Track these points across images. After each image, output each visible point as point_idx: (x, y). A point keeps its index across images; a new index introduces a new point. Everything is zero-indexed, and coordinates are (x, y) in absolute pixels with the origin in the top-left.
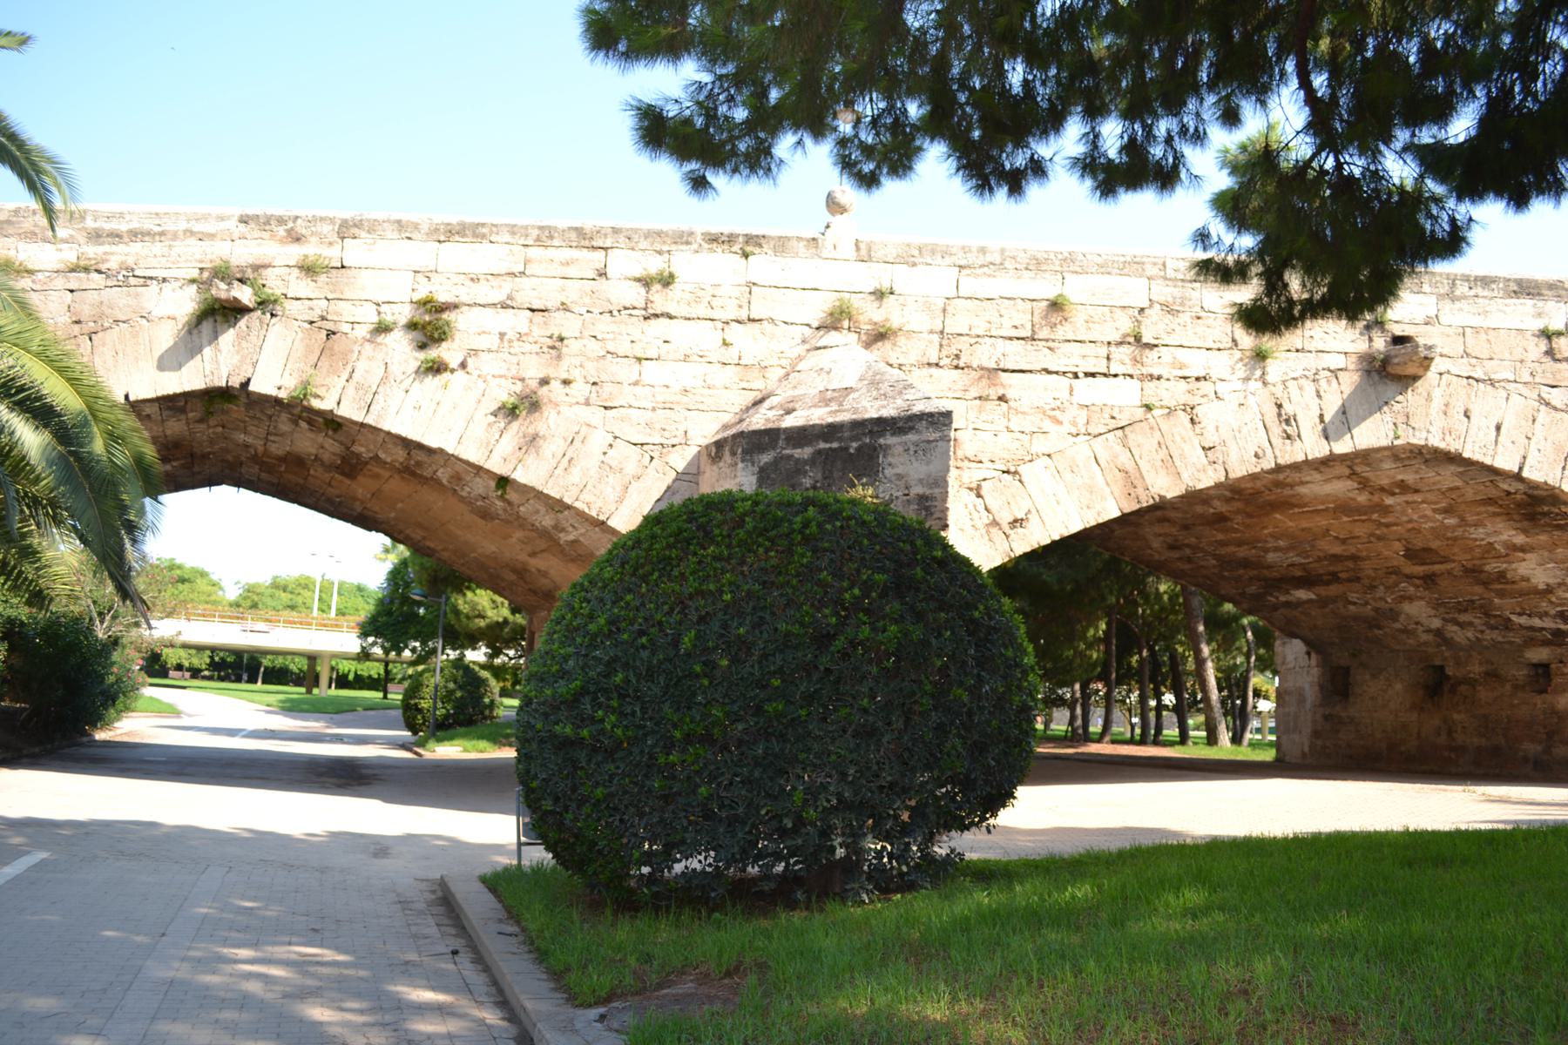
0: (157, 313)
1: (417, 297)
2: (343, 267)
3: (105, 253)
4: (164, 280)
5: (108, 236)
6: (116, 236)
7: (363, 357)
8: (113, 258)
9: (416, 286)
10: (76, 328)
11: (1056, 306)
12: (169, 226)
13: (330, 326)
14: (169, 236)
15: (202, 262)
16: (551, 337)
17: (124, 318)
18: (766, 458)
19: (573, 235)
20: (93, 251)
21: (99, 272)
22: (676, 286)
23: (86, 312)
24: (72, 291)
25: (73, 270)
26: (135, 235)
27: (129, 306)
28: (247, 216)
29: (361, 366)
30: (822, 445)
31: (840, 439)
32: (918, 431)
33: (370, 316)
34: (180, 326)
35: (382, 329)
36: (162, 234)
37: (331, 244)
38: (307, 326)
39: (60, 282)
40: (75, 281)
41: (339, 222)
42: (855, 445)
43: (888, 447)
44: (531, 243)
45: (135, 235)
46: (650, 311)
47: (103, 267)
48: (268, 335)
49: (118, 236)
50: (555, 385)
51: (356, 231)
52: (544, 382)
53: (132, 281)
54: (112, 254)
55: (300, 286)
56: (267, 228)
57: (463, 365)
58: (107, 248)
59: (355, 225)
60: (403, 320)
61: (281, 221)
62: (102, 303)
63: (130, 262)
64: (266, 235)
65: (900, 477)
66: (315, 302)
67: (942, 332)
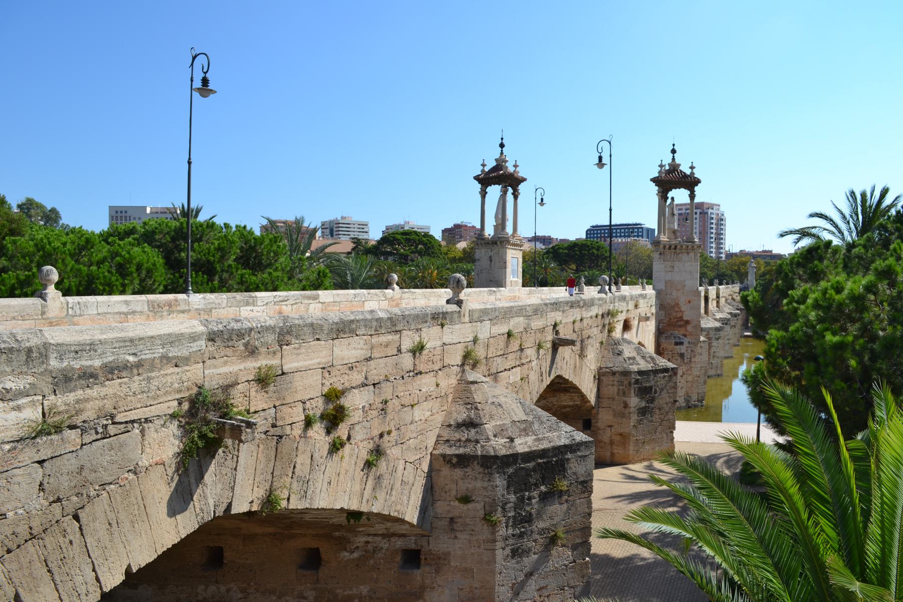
0: (144, 462)
1: (326, 390)
2: (283, 374)
3: (78, 402)
4: (147, 420)
5: (80, 377)
6: (89, 376)
7: (299, 452)
8: (89, 406)
9: (324, 382)
10: (57, 508)
11: (509, 335)
12: (147, 356)
13: (277, 431)
14: (146, 367)
15: (179, 391)
16: (382, 403)
17: (110, 479)
18: (511, 470)
19: (389, 324)
20: (61, 401)
21: (72, 427)
22: (425, 352)
23: (64, 484)
24: (41, 462)
25: (40, 433)
26: (113, 371)
27: (112, 462)
28: (214, 333)
29: (299, 460)
30: (540, 461)
31: (548, 457)
32: (582, 451)
33: (299, 416)
34: (170, 471)
35: (308, 423)
36: (139, 365)
37: (274, 353)
38: (263, 436)
39: (29, 455)
40: (45, 447)
41: (278, 330)
42: (554, 459)
43: (568, 459)
44: (373, 333)
45: (113, 371)
46: (416, 372)
47: (78, 421)
48: (240, 454)
49: (93, 376)
50: (386, 436)
51: (288, 338)
52: (381, 436)
53: (112, 430)
54: (87, 400)
55: (259, 400)
56: (230, 344)
57: (349, 438)
58: (80, 392)
59: (289, 333)
60: (318, 414)
61: (240, 334)
62: (82, 468)
63: (109, 405)
64: (229, 352)
65: (575, 473)
66: (268, 411)
67: (486, 358)
